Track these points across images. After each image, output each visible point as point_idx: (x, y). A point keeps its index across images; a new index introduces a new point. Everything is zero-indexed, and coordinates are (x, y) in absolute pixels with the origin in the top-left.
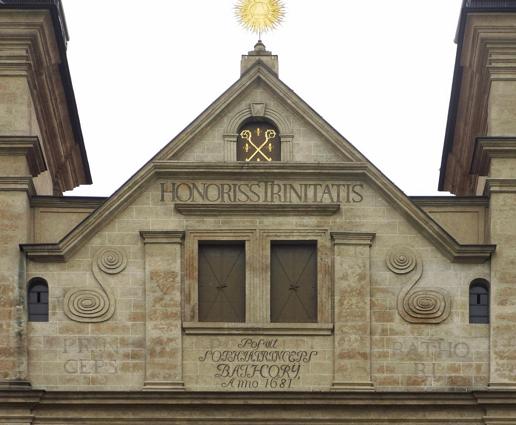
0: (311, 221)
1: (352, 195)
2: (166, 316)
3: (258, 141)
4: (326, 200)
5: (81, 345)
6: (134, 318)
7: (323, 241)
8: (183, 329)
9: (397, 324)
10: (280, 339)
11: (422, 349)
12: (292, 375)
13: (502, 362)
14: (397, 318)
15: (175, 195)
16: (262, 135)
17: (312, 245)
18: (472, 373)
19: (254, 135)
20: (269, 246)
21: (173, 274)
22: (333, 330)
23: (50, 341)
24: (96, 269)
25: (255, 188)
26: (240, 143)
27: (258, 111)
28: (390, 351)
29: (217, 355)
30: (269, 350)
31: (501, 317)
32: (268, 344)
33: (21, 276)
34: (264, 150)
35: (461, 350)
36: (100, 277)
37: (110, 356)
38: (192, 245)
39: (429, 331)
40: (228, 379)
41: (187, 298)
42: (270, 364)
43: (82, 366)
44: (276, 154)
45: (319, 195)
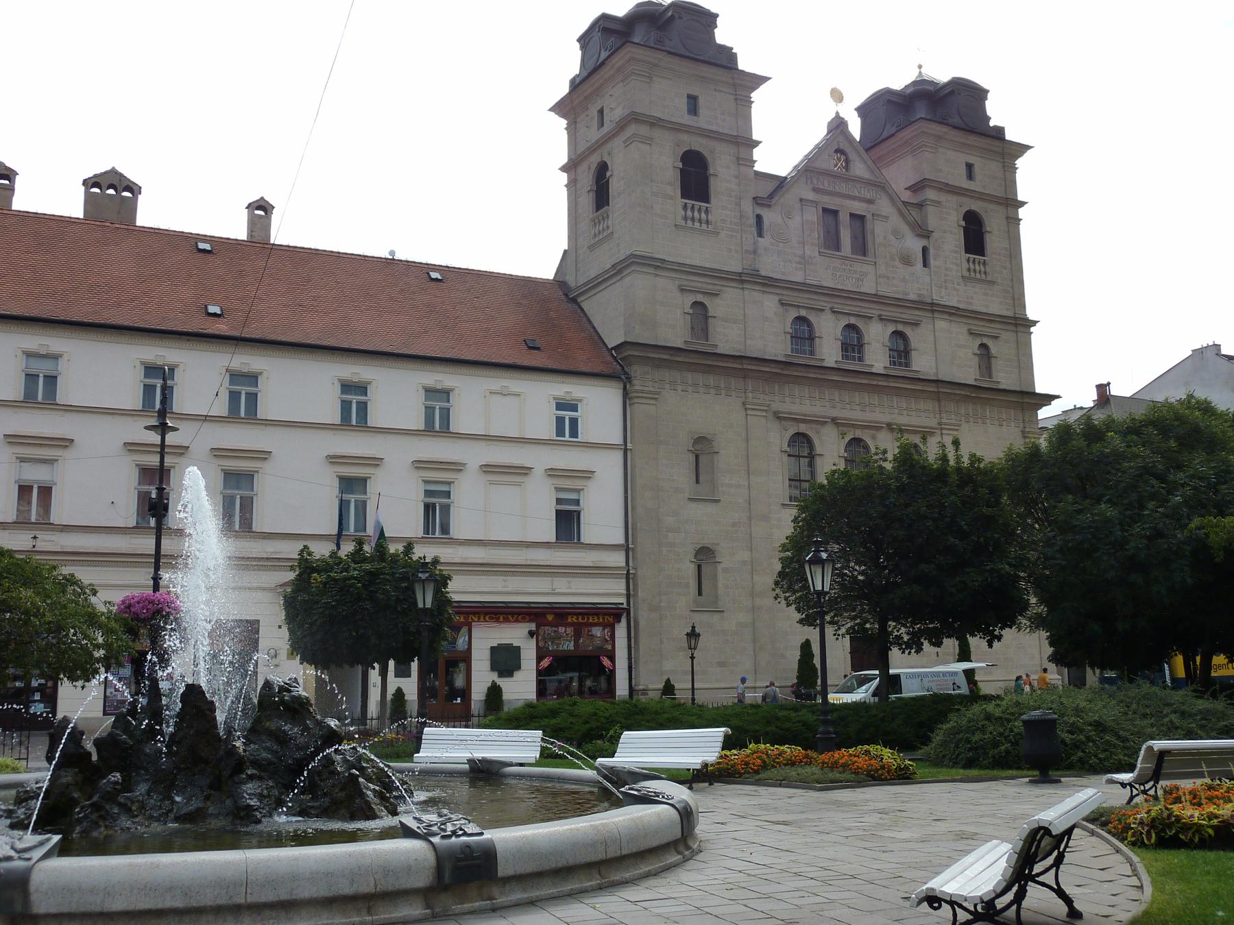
0: (864, 205)
7: (869, 217)
8: (819, 252)
9: (897, 263)
10: (855, 263)
11: (907, 277)
14: (898, 260)
15: (812, 182)
20: (848, 214)
25: (842, 184)
27: (842, 147)
28: (896, 276)
33: (753, 212)
36: (786, 219)
37: (790, 261)
39: (910, 268)
40: (837, 282)
44: (847, 168)
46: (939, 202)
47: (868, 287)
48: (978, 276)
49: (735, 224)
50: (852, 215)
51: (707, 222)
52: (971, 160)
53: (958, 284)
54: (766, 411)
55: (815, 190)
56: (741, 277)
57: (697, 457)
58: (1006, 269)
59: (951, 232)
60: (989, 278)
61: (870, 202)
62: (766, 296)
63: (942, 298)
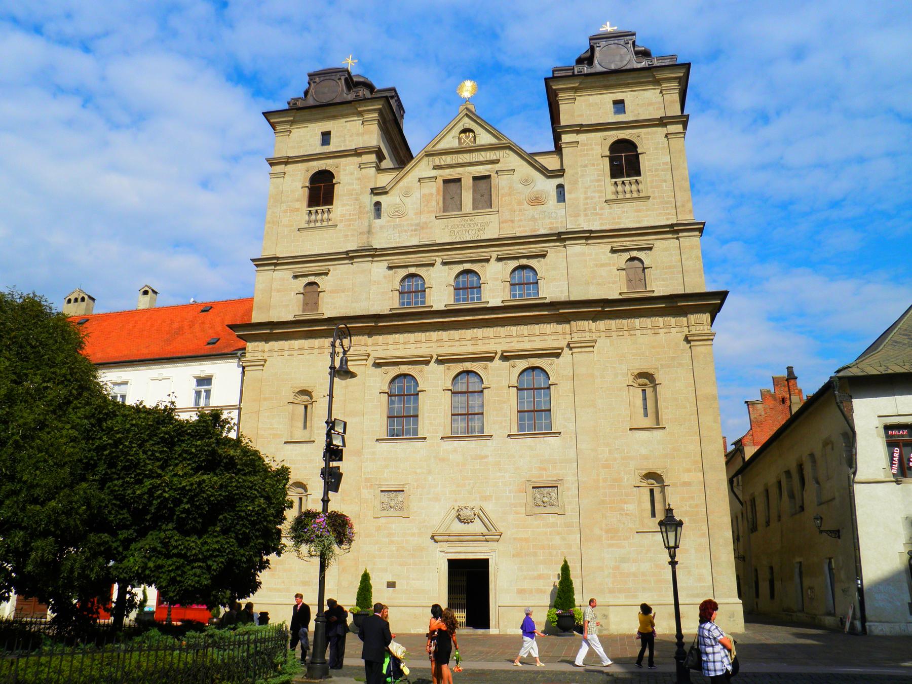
1: (505, 155)
2: (429, 212)
3: (467, 137)
4: (495, 158)
5: (394, 227)
6: (416, 214)
7: (493, 175)
8: (436, 217)
9: (526, 206)
12: (482, 232)
13: (571, 219)
16: (469, 135)
17: (489, 177)
18: (559, 225)
19: (466, 136)
20: (471, 179)
21: (431, 194)
22: (498, 211)
23: (381, 227)
24: (401, 195)
26: (460, 139)
27: (467, 126)
28: (523, 218)
29: (450, 227)
30: (472, 222)
31: (570, 199)
32: (471, 220)
33: (371, 201)
34: (470, 141)
35: (554, 215)
36: (403, 198)
37: (406, 231)
38: (440, 181)
40: (455, 237)
41: (438, 204)
42: (472, 228)
43: (394, 236)
45: (492, 156)
46: (578, 142)
47: (491, 233)
48: (628, 196)
49: (353, 215)
50: (476, 179)
51: (329, 220)
52: (619, 96)
53: (602, 208)
54: (366, 360)
55: (435, 168)
56: (348, 254)
57: (306, 407)
58: (665, 181)
59: (593, 165)
60: (641, 195)
61: (496, 162)
62: (375, 264)
63: (579, 225)
